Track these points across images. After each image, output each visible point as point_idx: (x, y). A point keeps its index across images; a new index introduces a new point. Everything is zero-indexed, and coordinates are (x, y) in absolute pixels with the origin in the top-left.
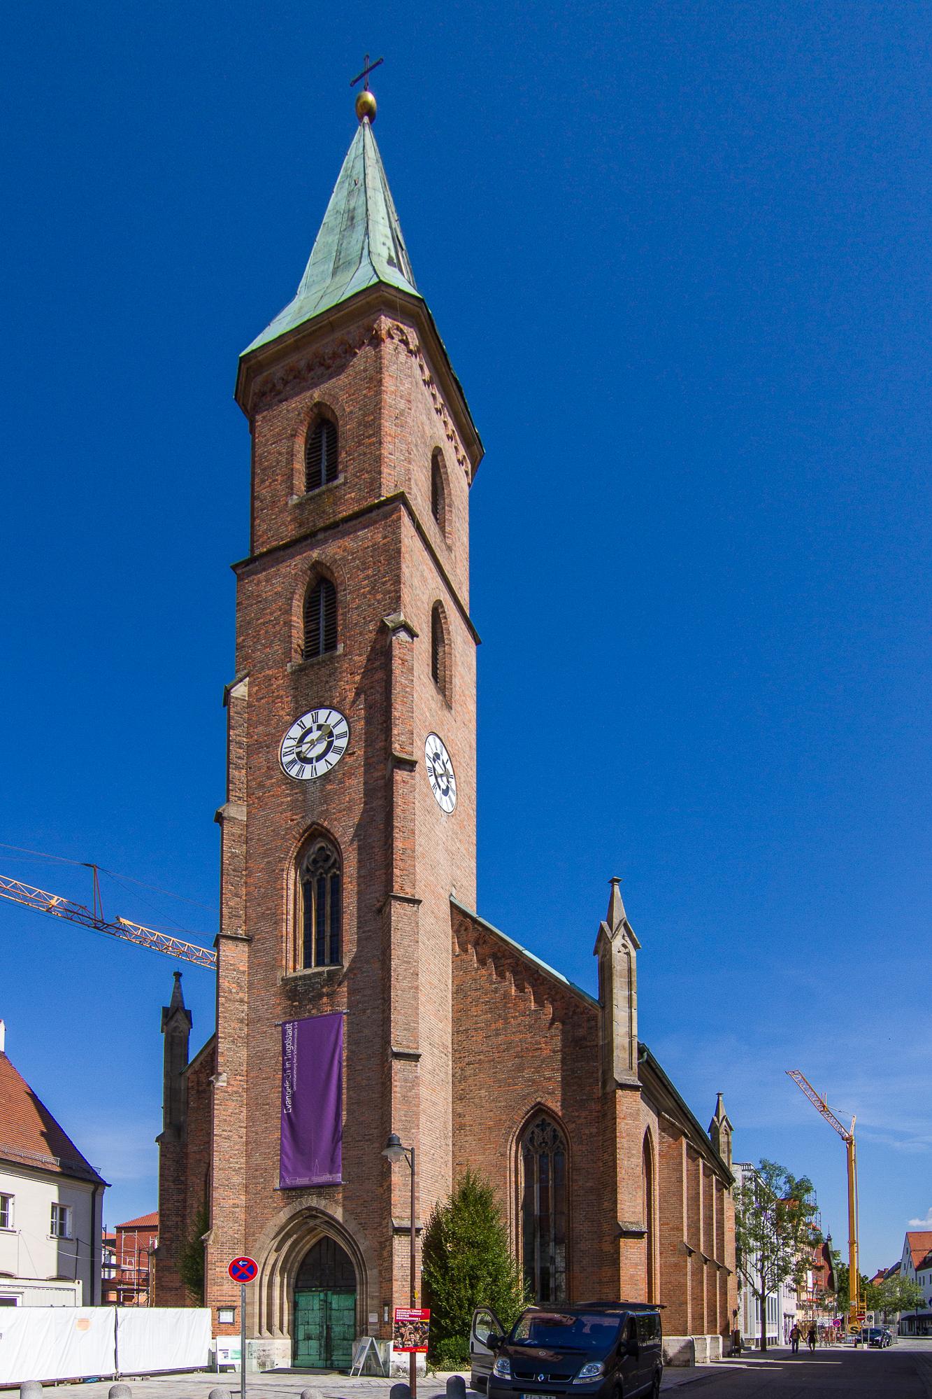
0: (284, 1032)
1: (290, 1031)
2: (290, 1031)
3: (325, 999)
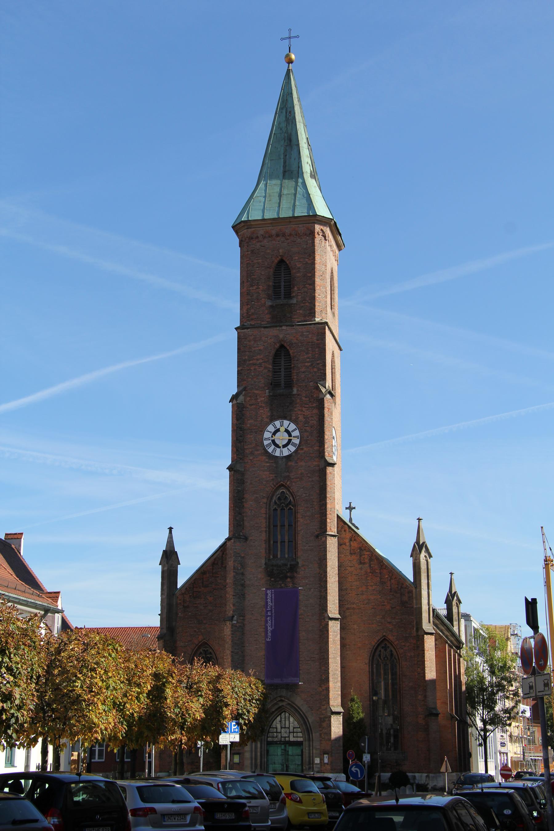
0: (267, 594)
1: (269, 595)
2: (269, 595)
3: (289, 580)
